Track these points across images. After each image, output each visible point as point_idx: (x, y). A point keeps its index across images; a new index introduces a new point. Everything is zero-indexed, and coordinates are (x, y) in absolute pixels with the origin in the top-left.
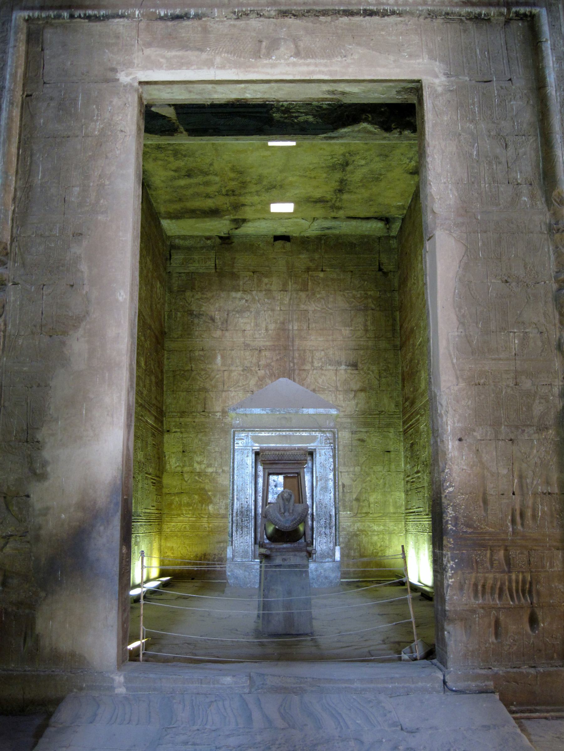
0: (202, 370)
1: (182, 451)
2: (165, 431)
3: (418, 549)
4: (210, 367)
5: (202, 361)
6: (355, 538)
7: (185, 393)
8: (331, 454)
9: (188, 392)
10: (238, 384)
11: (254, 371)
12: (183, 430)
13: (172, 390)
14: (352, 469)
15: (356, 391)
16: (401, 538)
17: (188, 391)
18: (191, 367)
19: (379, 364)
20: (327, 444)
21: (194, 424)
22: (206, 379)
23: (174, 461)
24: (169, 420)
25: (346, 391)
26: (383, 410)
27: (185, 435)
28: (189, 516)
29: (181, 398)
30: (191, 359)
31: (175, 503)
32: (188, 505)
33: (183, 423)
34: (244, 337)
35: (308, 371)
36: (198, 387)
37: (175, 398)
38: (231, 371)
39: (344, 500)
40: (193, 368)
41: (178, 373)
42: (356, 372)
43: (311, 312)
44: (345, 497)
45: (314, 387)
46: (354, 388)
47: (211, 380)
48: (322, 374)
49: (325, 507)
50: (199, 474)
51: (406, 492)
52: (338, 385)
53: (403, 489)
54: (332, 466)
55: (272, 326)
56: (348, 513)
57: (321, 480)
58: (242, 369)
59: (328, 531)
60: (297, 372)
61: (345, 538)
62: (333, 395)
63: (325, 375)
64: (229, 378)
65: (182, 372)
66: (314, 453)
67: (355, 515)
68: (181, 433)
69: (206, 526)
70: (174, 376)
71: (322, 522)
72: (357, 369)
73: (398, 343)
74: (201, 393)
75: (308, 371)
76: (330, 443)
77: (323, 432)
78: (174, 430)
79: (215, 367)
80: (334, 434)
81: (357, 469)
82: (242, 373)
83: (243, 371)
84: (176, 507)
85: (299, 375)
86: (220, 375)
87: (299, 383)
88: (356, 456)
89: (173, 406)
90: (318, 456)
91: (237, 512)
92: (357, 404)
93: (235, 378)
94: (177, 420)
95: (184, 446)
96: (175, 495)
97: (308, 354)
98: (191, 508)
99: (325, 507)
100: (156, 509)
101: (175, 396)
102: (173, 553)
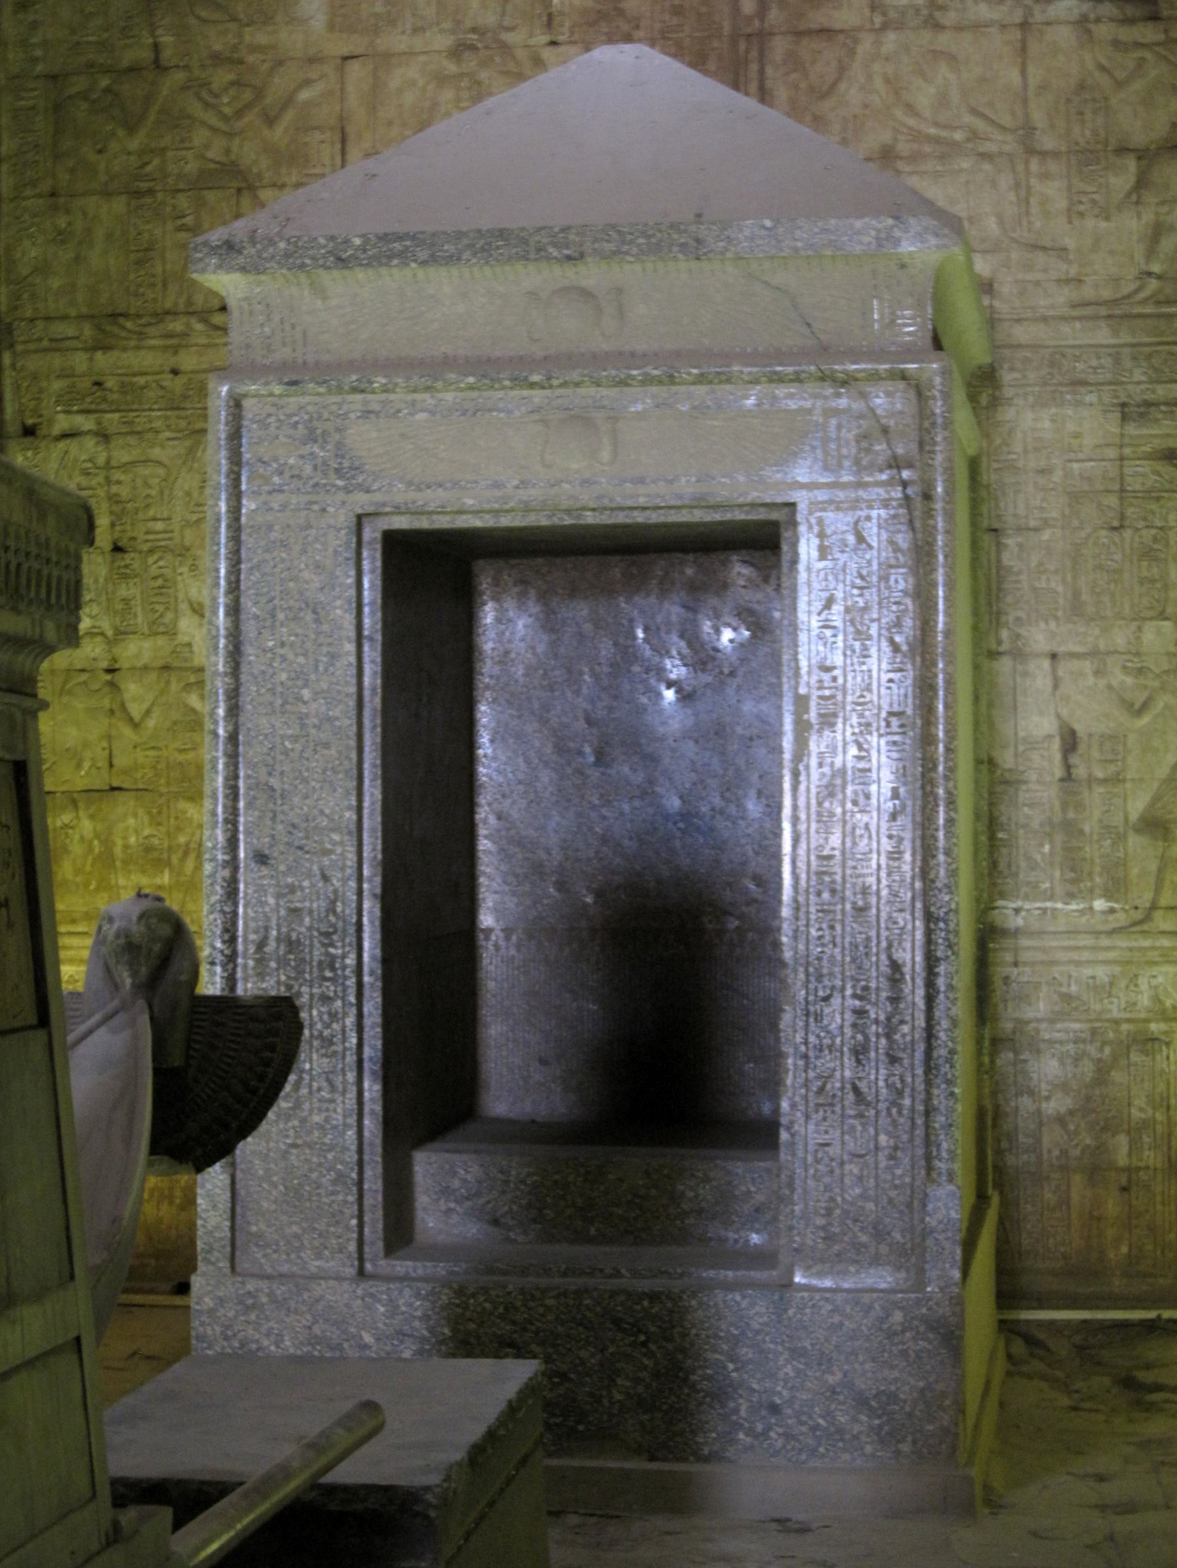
0: (218, 59)
2: (12, 428)
4: (262, 38)
6: (1135, 1057)
7: (119, 205)
8: (903, 540)
9: (138, 194)
11: (521, 54)
12: (112, 419)
13: (46, 186)
14: (1120, 638)
15: (1141, 154)
17: (138, 191)
18: (156, 47)
20: (871, 468)
21: (178, 384)
22: (239, 113)
24: (33, 363)
25: (1089, 157)
27: (122, 455)
29: (99, 233)
31: (77, 849)
33: (110, 383)
35: (850, 35)
36: (192, 167)
37: (62, 237)
38: (384, 60)
39: (1071, 829)
40: (167, 54)
41: (79, 84)
42: (1148, 33)
44: (1079, 806)
45: (886, 137)
46: (1139, 138)
47: (270, 121)
48: (936, 54)
49: (861, 911)
52: (1038, 117)
54: (908, 622)
56: (1099, 904)
57: (828, 721)
58: (443, 42)
59: (877, 1077)
60: (779, 46)
61: (1077, 1060)
62: (1005, 181)
63: (952, 58)
65: (104, 82)
66: (786, 534)
67: (1142, 922)
68: (104, 437)
70: (57, 108)
71: (837, 1014)
72: (1155, 18)
74: (210, 196)
75: (850, 35)
76: (895, 463)
77: (847, 381)
78: (62, 423)
79: (290, 40)
80: (920, 392)
81: (1156, 637)
82: (452, 68)
83: (458, 51)
85: (794, 62)
87: (795, 111)
88: (1148, 554)
89: (55, 283)
90: (807, 548)
91: (261, 945)
92: (1157, 232)
93: (409, 98)
94: (80, 361)
96: (74, 804)
99: (861, 911)
101: (62, 222)
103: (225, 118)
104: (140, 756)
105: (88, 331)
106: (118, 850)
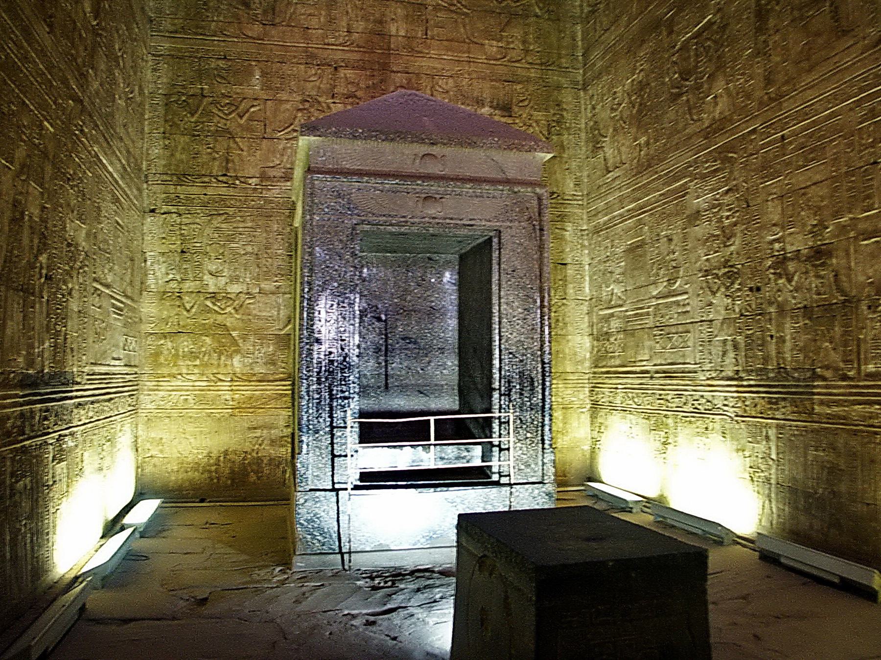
1: (179, 251)
3: (665, 443)
4: (238, 91)
5: (222, 78)
7: (187, 139)
9: (194, 136)
10: (292, 127)
16: (583, 416)
19: (546, 110)
22: (230, 113)
23: (163, 270)
26: (555, 190)
28: (193, 377)
30: (200, 75)
32: (193, 355)
34: (307, 38)
43: (430, 8)
47: (241, 117)
50: (214, 296)
51: (601, 337)
53: (589, 330)
55: (360, 26)
64: (276, 111)
69: (228, 397)
72: (511, 116)
73: (580, 78)
78: (165, 208)
84: (166, 360)
86: (258, 108)
94: (172, 189)
95: (184, 239)
96: (165, 337)
97: (425, 82)
98: (198, 362)
100: (126, 365)
101: (167, 142)
102: (161, 451)
103: (226, 114)
104: (189, 320)
105: (175, 178)
106: (181, 353)
